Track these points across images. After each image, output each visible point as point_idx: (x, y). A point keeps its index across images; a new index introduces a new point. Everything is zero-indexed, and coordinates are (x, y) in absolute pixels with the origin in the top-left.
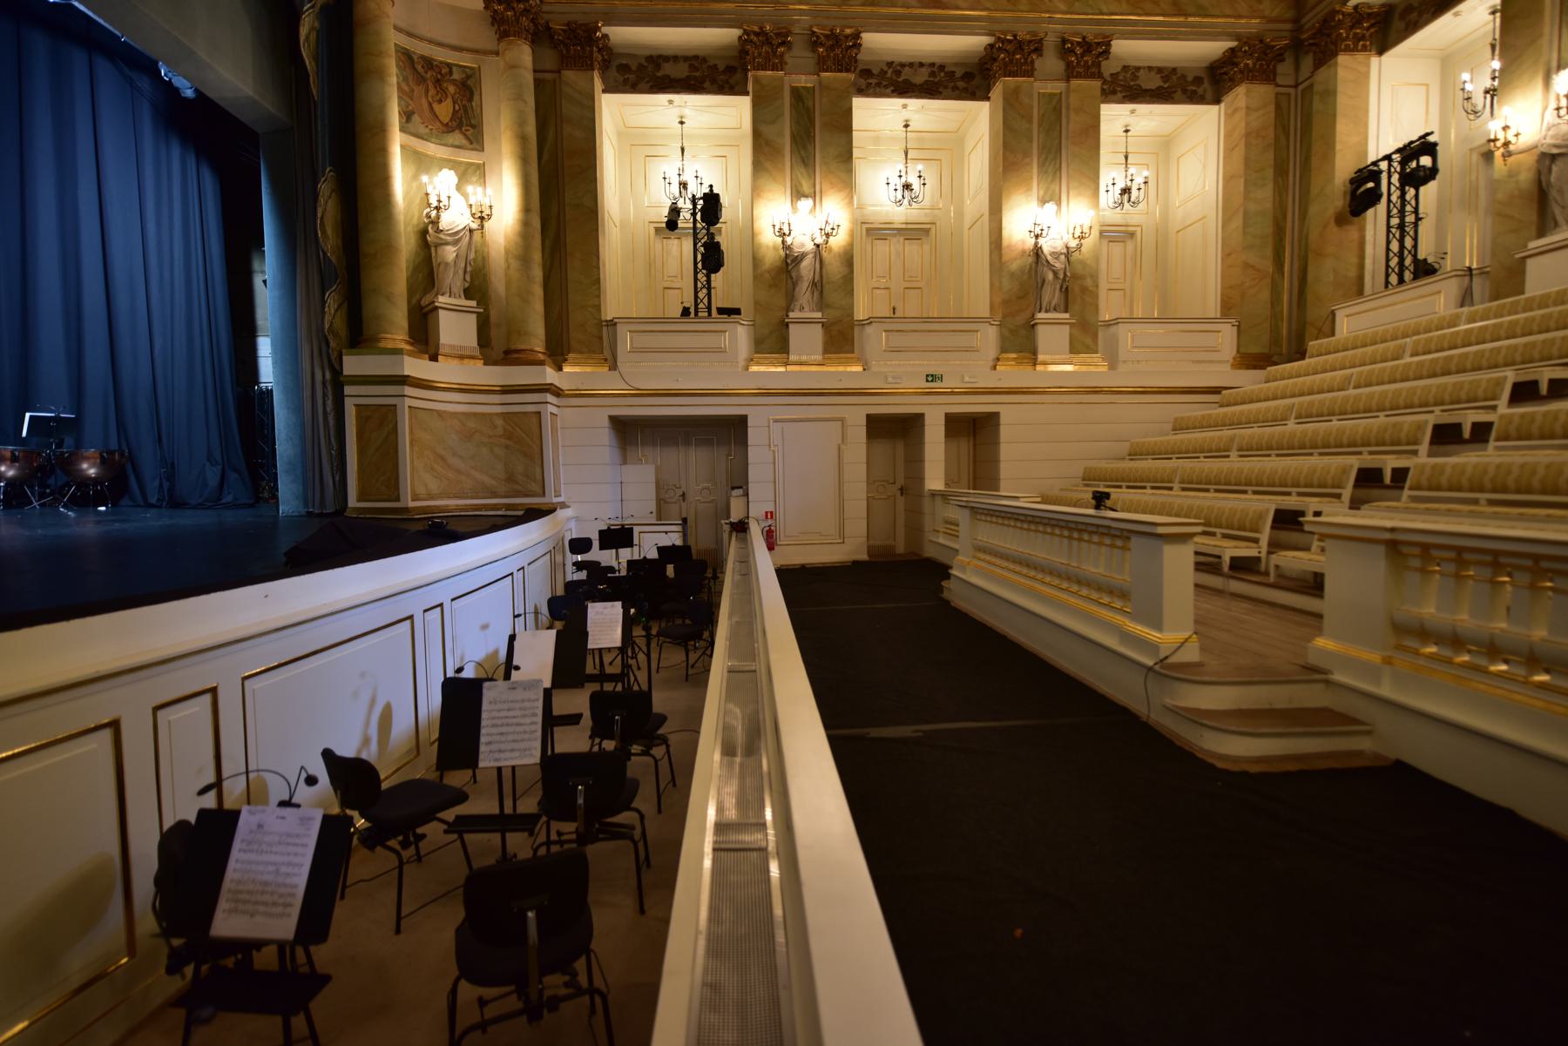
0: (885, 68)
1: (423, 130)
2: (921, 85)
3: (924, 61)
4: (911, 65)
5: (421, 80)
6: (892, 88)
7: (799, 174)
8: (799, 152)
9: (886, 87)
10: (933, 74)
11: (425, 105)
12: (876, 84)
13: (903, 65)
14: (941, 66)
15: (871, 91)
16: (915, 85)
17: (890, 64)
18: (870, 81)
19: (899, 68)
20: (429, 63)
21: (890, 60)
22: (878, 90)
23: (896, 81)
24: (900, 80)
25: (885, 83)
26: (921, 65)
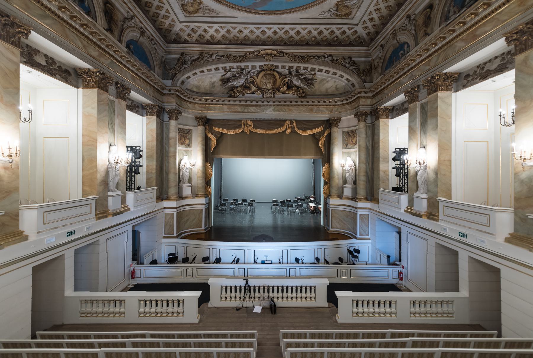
0: (476, 69)
1: (350, 147)
2: (496, 69)
3: (497, 55)
4: (490, 61)
5: (350, 136)
6: (479, 78)
7: (423, 138)
8: (423, 129)
9: (476, 79)
10: (504, 59)
11: (351, 141)
12: (471, 80)
13: (485, 63)
14: (508, 52)
15: (469, 83)
16: (492, 71)
17: (478, 67)
18: (468, 80)
19: (483, 66)
20: (352, 131)
21: (478, 64)
22: (472, 82)
23: (482, 73)
24: (484, 72)
25: (475, 77)
26: (496, 57)
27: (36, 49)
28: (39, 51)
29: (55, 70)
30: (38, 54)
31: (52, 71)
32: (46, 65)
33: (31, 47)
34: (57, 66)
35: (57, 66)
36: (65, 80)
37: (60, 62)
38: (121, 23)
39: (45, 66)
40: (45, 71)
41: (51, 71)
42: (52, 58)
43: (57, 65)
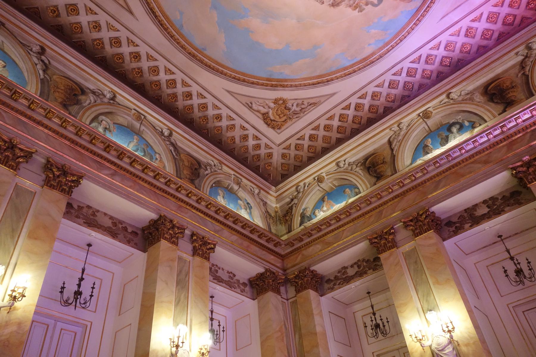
27: (473, 206)
28: (476, 205)
29: (500, 205)
30: (477, 208)
31: (498, 210)
32: (489, 209)
33: (468, 208)
34: (500, 200)
35: (500, 200)
36: (517, 205)
37: (499, 194)
38: (520, 75)
39: (488, 212)
40: (491, 217)
41: (497, 211)
42: (491, 197)
43: (500, 198)
